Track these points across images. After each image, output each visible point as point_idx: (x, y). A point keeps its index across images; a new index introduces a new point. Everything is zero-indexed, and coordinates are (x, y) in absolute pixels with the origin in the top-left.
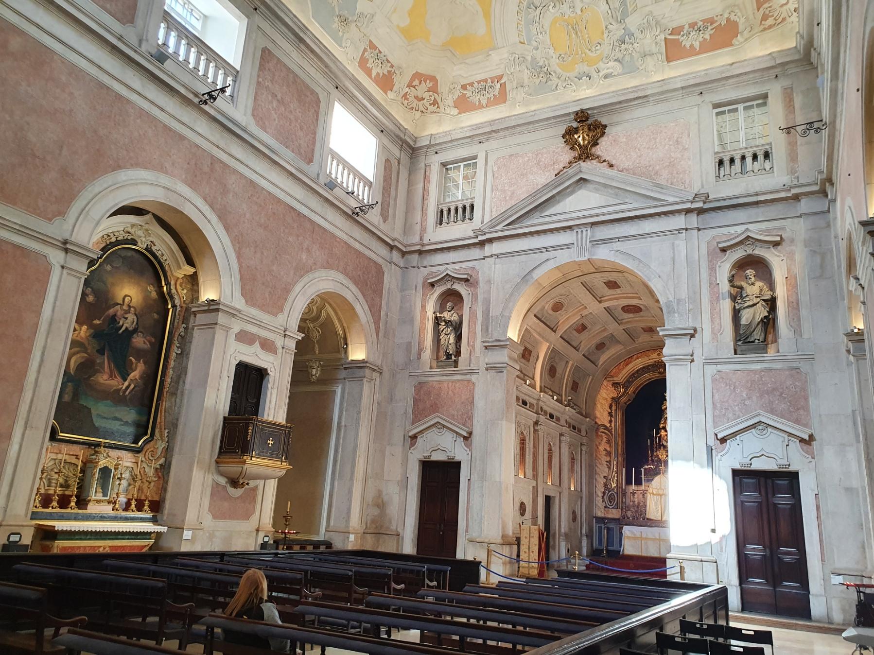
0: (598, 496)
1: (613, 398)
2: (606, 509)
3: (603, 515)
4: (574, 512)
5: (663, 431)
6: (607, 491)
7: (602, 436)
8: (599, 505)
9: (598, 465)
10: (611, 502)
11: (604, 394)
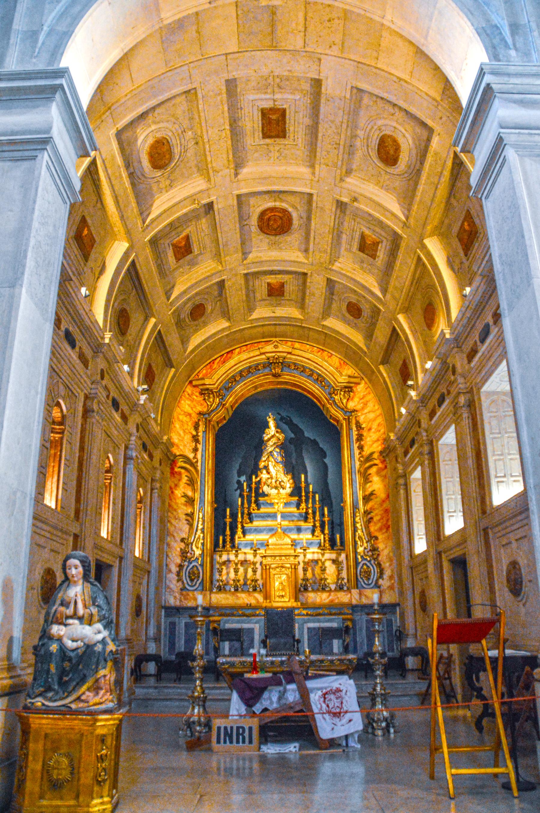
0: (170, 571)
1: (200, 413)
2: (184, 593)
3: (178, 603)
4: (139, 599)
5: (264, 472)
6: (186, 563)
7: (180, 474)
8: (172, 586)
9: (173, 521)
10: (192, 580)
11: (187, 406)
